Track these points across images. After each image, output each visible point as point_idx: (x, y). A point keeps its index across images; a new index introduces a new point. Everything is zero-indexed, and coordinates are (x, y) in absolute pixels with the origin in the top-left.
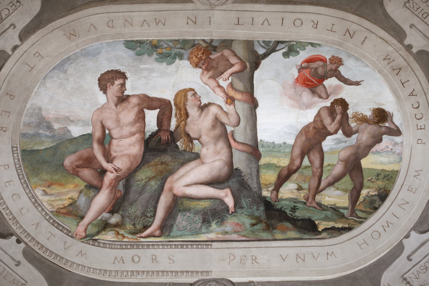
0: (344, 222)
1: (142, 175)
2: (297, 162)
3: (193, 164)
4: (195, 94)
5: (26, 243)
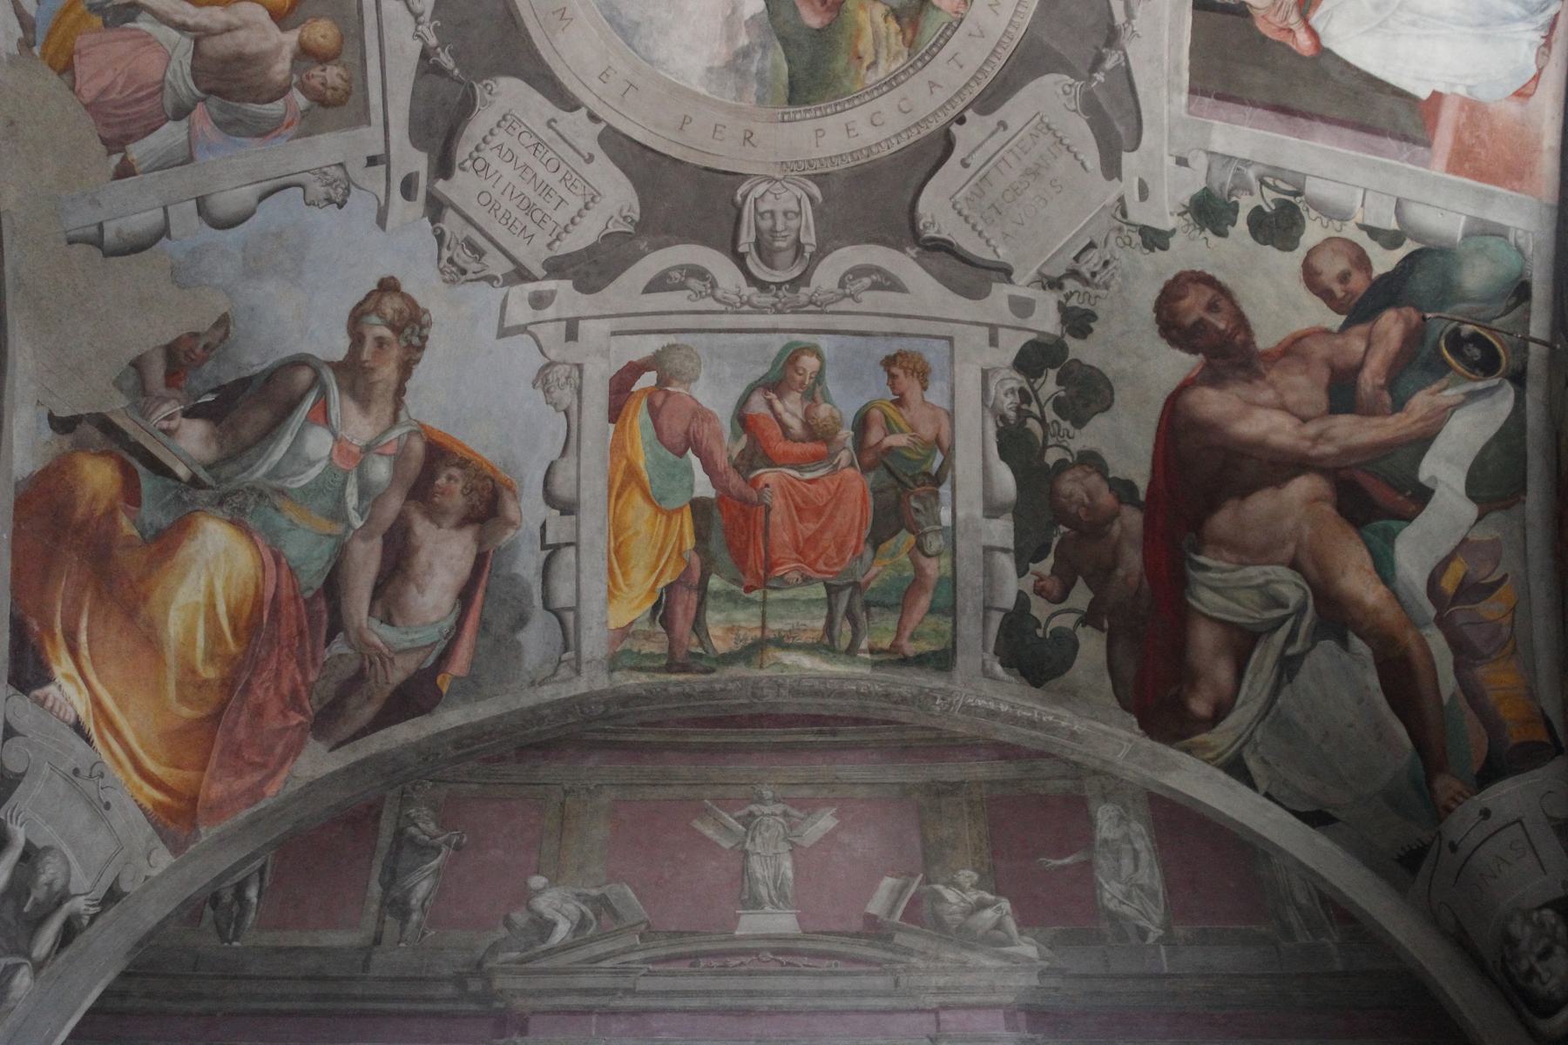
5: (966, 108)
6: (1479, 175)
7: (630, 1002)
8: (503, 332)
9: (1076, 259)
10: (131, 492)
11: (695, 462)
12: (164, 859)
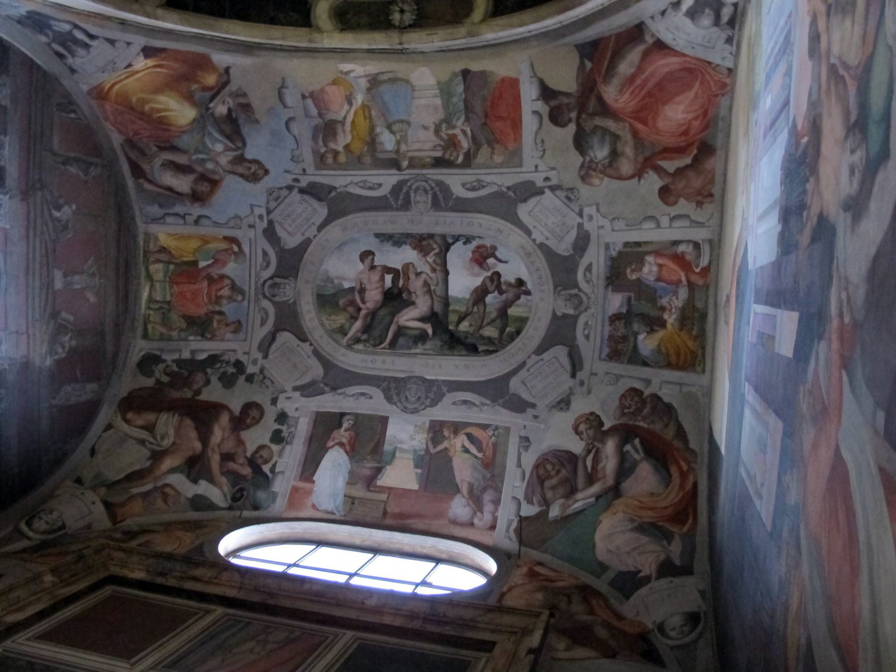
0: (494, 347)
1: (383, 312)
2: (470, 310)
3: (411, 307)
4: (413, 266)
6: (291, 495)
7: (31, 234)
8: (252, 206)
9: (269, 378)
10: (205, 89)
11: (210, 262)
12: (85, 88)
